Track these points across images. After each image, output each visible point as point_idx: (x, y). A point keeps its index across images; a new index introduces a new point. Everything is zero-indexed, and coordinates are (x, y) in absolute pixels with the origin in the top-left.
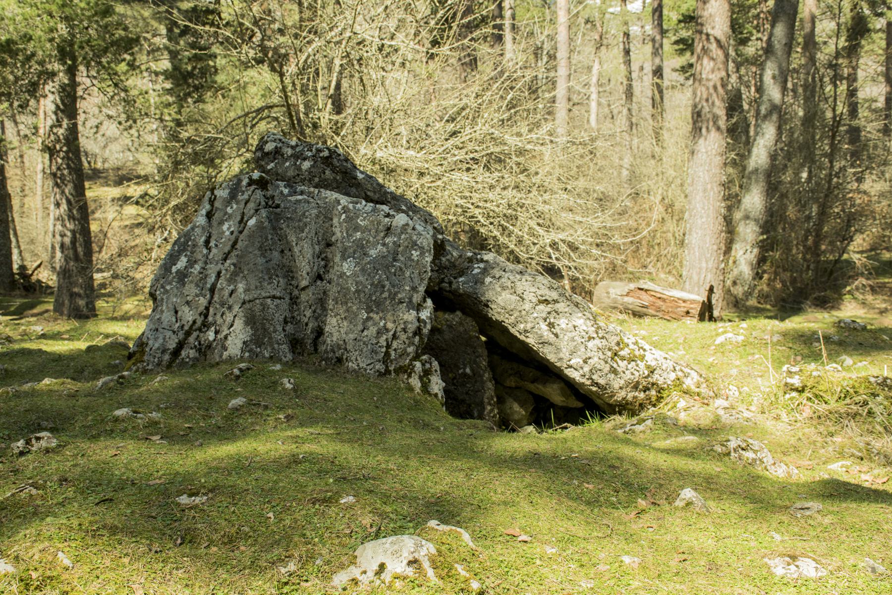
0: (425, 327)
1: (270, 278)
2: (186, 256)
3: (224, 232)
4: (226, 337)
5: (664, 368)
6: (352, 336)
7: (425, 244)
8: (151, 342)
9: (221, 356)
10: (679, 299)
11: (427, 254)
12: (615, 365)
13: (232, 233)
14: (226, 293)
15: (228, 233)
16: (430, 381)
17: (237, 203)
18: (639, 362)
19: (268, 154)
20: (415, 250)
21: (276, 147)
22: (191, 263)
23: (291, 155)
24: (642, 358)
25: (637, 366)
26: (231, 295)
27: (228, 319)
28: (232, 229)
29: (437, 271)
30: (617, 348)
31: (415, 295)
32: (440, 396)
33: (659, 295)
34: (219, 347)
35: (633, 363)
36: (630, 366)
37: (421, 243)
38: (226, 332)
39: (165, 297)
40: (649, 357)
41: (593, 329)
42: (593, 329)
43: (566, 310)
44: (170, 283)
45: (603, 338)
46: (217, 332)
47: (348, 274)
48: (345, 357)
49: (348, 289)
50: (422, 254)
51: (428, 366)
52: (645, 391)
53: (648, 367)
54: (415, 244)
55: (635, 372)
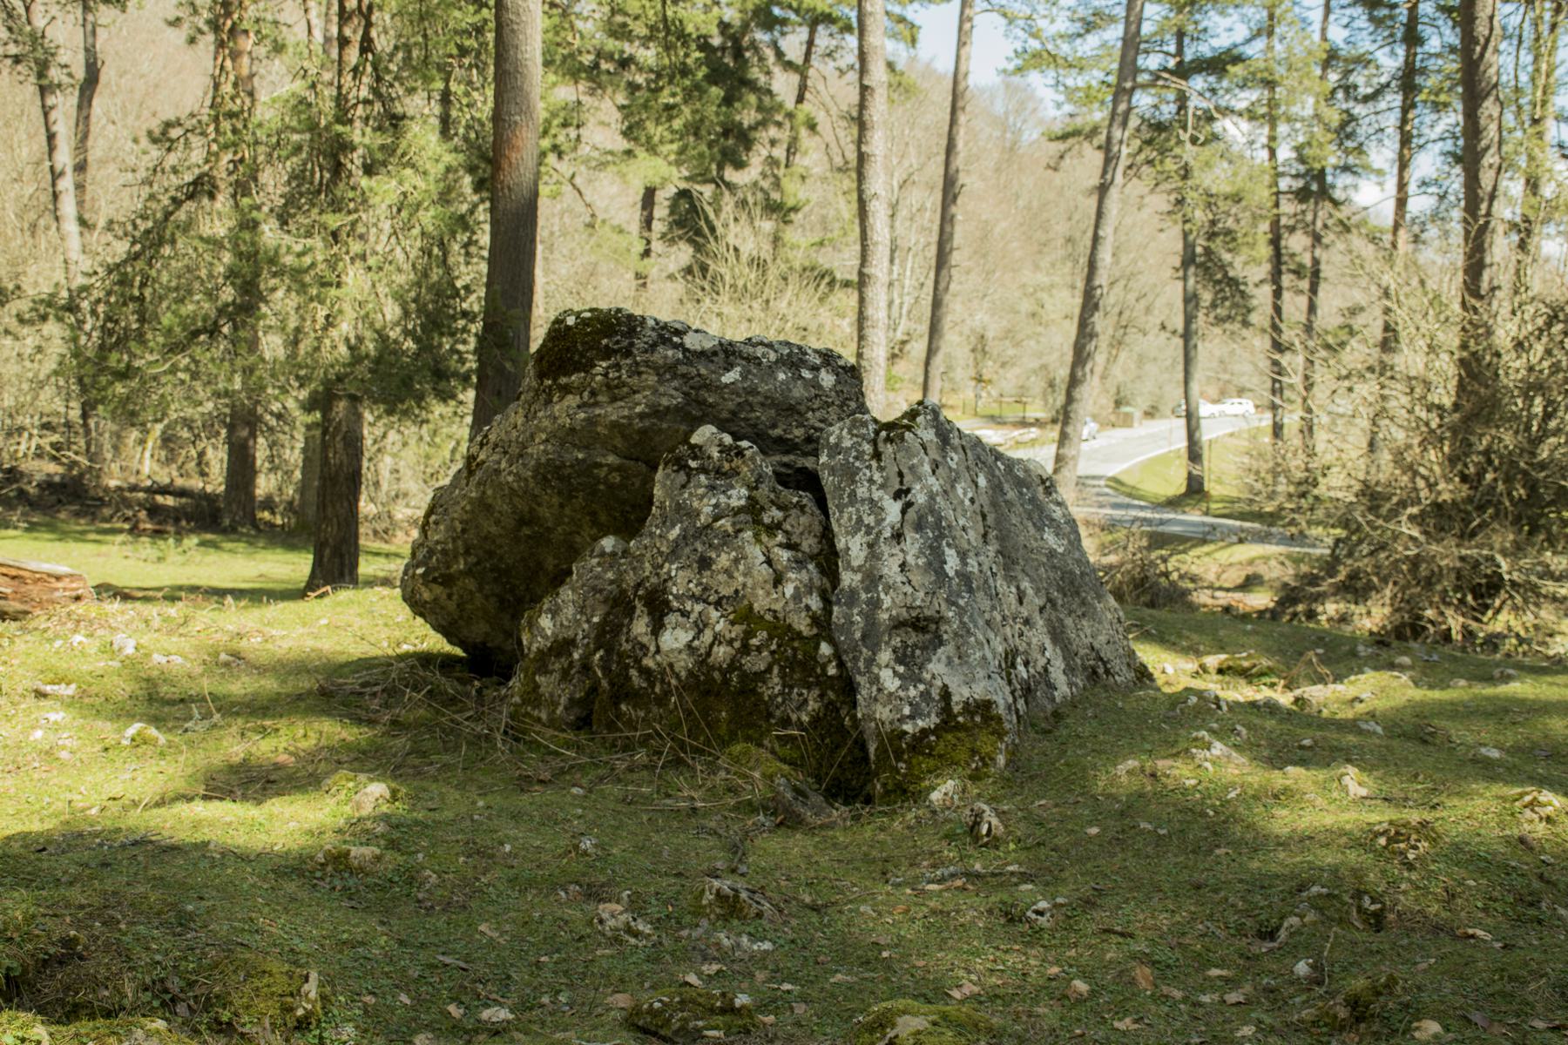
2: (949, 545)
3: (962, 502)
4: (1046, 670)
6: (1102, 638)
8: (995, 698)
9: (1053, 699)
10: (49, 575)
13: (972, 500)
14: (1013, 599)
15: (967, 503)
17: (954, 449)
19: (702, 354)
21: (721, 344)
22: (963, 556)
23: (777, 362)
26: (1021, 603)
27: (1034, 641)
28: (970, 495)
33: (14, 572)
34: (1043, 685)
38: (1042, 662)
39: (966, 619)
44: (959, 596)
46: (1026, 664)
47: (1061, 550)
48: (1101, 671)
49: (1071, 572)
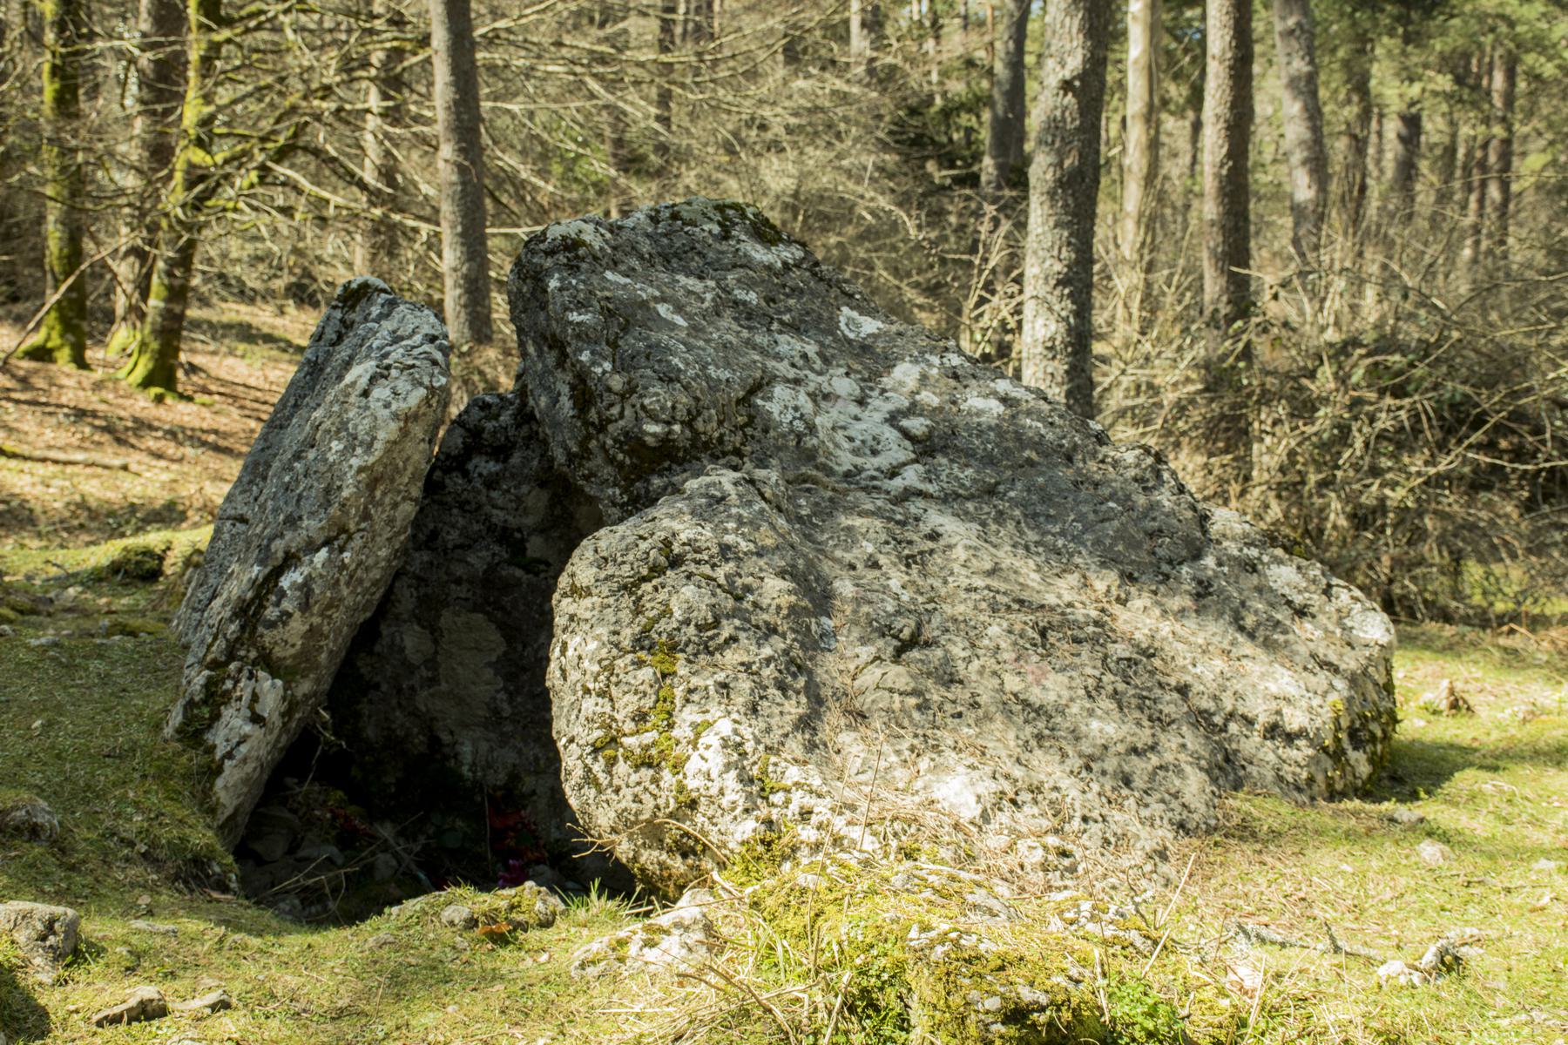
0: (278, 604)
1: (251, 482)
5: (725, 802)
7: (363, 427)
11: (359, 451)
12: (598, 768)
16: (216, 717)
18: (666, 775)
20: (339, 439)
24: (677, 767)
25: (655, 781)
29: (622, 505)
30: (629, 726)
31: (289, 535)
32: (218, 754)
35: (646, 773)
36: (634, 778)
37: (356, 426)
40: (693, 765)
41: (596, 668)
42: (596, 668)
43: (588, 615)
45: (602, 694)
50: (349, 449)
51: (229, 684)
52: (685, 856)
53: (681, 789)
54: (343, 425)
55: (646, 797)
